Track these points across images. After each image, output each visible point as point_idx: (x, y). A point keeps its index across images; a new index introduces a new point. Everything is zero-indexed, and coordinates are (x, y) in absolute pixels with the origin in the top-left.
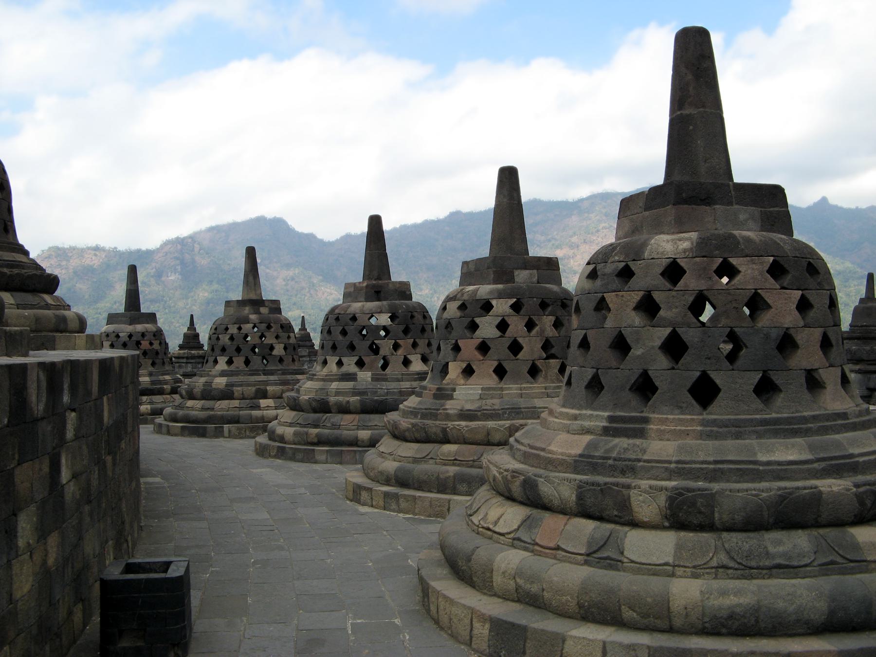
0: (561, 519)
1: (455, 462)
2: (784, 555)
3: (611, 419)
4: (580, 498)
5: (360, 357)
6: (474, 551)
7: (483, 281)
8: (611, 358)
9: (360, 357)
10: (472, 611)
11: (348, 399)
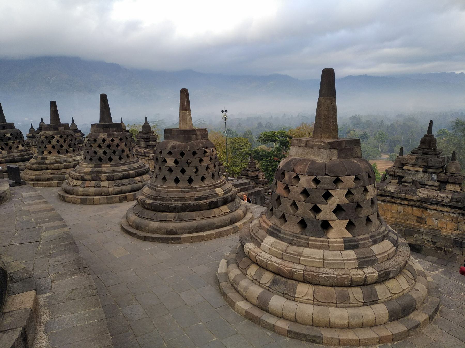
0: (89, 182)
1: (51, 174)
2: (124, 183)
3: (95, 165)
4: (92, 178)
5: (2, 147)
6: (73, 189)
7: (50, 130)
8: (94, 155)
9: (2, 147)
10: (76, 198)
11: (1, 159)
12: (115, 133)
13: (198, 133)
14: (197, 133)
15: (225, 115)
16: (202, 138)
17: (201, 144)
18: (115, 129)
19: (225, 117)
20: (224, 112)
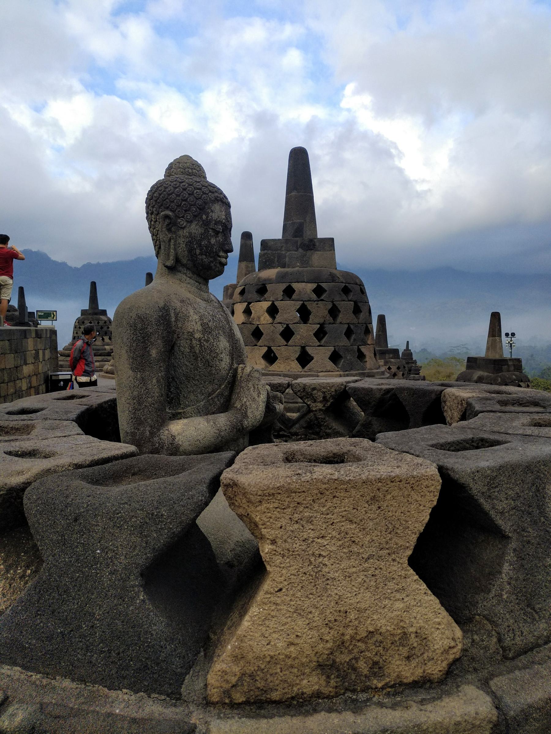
12: (392, 360)
13: (510, 363)
14: (509, 364)
15: (511, 341)
16: (514, 370)
17: (514, 377)
18: (391, 356)
19: (511, 344)
20: (510, 336)
